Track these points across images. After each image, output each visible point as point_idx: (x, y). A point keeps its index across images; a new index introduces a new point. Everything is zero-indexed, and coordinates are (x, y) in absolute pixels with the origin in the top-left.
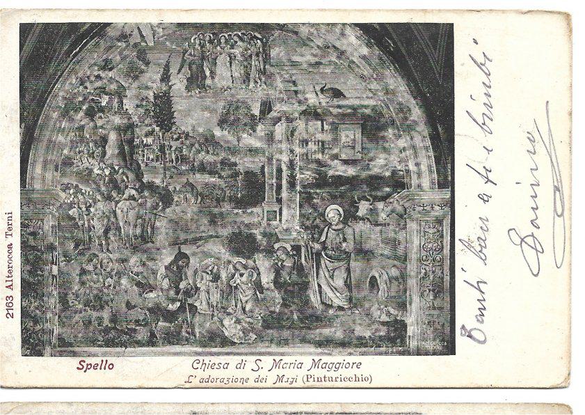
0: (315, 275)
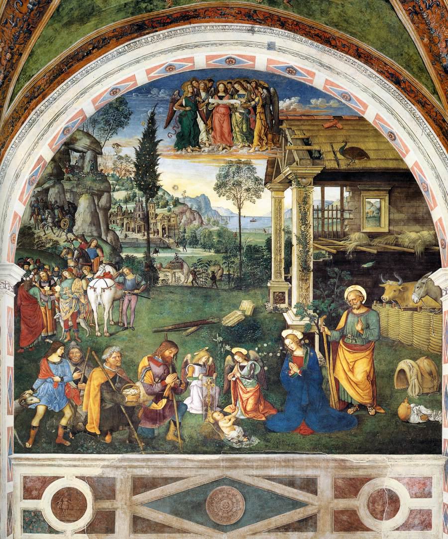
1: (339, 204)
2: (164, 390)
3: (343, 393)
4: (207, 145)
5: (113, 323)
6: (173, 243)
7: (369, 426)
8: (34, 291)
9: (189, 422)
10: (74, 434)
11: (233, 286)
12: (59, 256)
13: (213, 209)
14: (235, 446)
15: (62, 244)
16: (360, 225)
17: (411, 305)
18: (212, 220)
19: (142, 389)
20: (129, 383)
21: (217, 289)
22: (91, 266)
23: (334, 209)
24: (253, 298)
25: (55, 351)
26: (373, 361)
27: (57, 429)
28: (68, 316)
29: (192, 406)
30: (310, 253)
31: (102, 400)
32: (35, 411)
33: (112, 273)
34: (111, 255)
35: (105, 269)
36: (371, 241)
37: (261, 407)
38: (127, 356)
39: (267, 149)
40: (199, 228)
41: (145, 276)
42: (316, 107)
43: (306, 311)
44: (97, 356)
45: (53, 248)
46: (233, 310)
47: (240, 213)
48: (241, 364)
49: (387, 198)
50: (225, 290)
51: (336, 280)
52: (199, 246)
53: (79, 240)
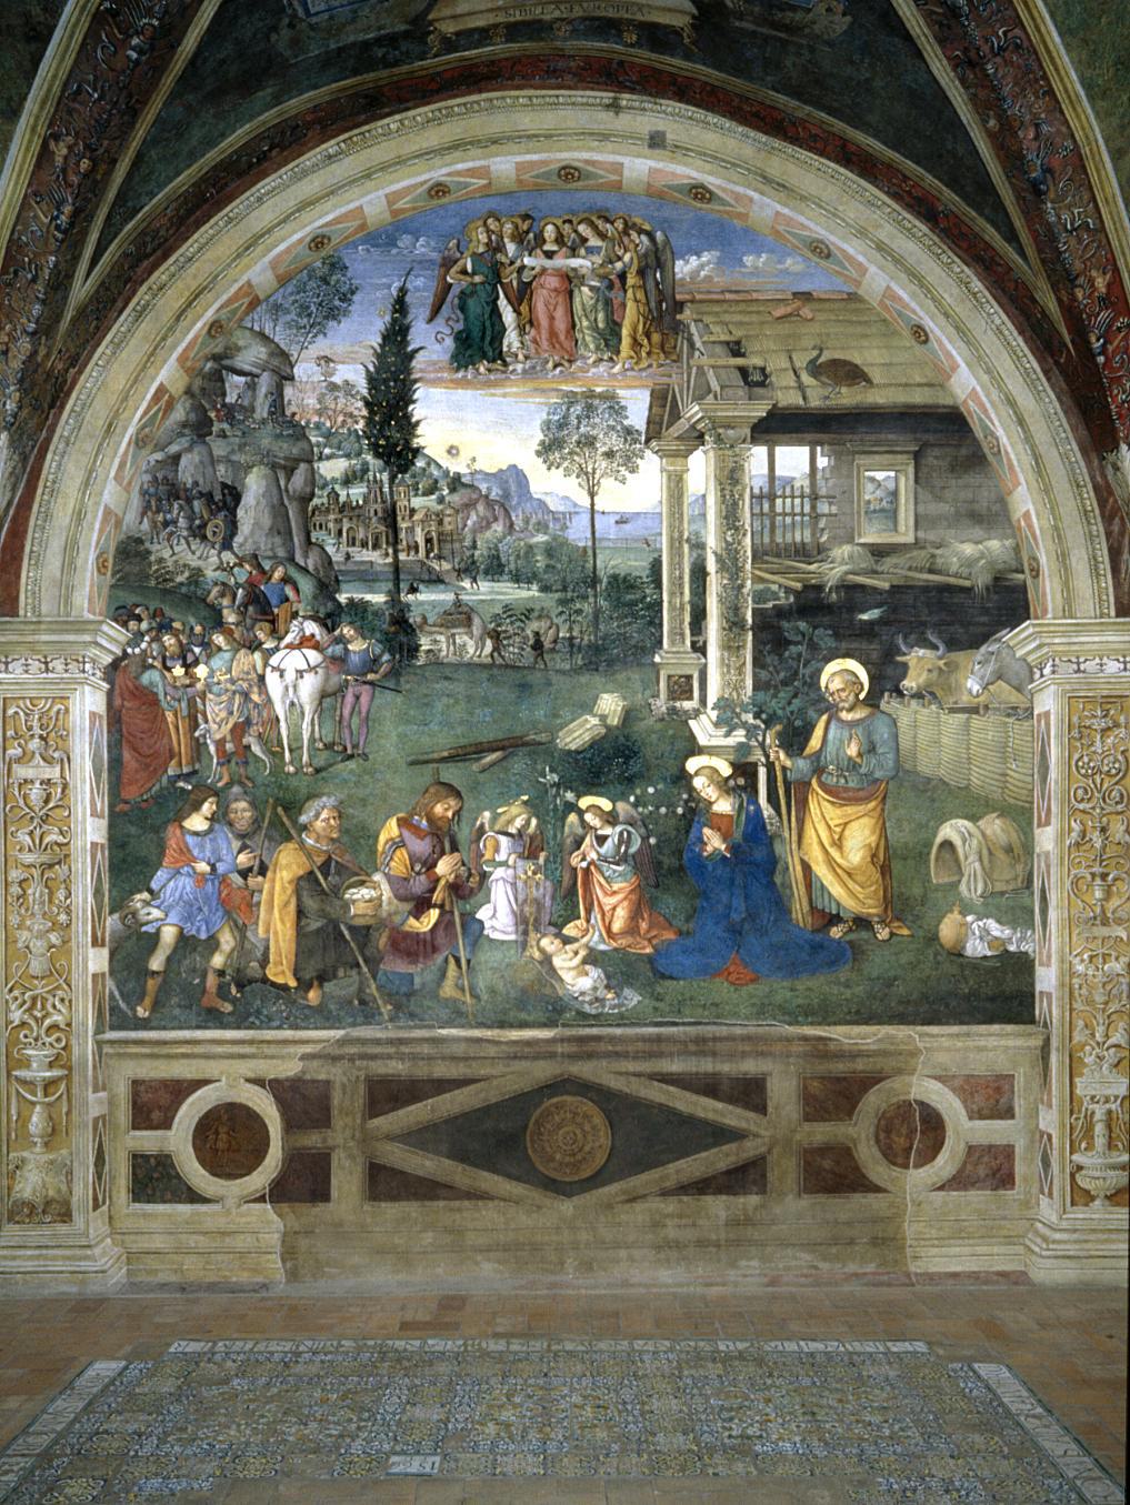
0: (794, 838)
1: (807, 483)
2: (432, 890)
3: (819, 893)
4: (521, 357)
5: (321, 746)
6: (448, 571)
7: (877, 963)
8: (149, 677)
9: (486, 957)
10: (240, 986)
11: (580, 662)
12: (204, 600)
13: (535, 496)
14: (587, 1009)
15: (210, 574)
17: (965, 700)
18: (533, 520)
19: (385, 887)
22: (273, 622)
23: (797, 493)
24: (619, 688)
25: (197, 807)
26: (884, 823)
27: (204, 976)
29: (494, 922)
30: (745, 591)
31: (301, 913)
32: (154, 940)
33: (318, 637)
34: (315, 597)
35: (302, 630)
36: (877, 562)
37: (644, 926)
38: (353, 817)
39: (650, 366)
40: (504, 537)
41: (389, 642)
42: (756, 272)
43: (738, 715)
44: (289, 817)
45: (189, 584)
46: (582, 715)
47: (593, 505)
48: (600, 832)
49: (911, 470)
50: (562, 672)
52: (506, 577)
53: (247, 567)
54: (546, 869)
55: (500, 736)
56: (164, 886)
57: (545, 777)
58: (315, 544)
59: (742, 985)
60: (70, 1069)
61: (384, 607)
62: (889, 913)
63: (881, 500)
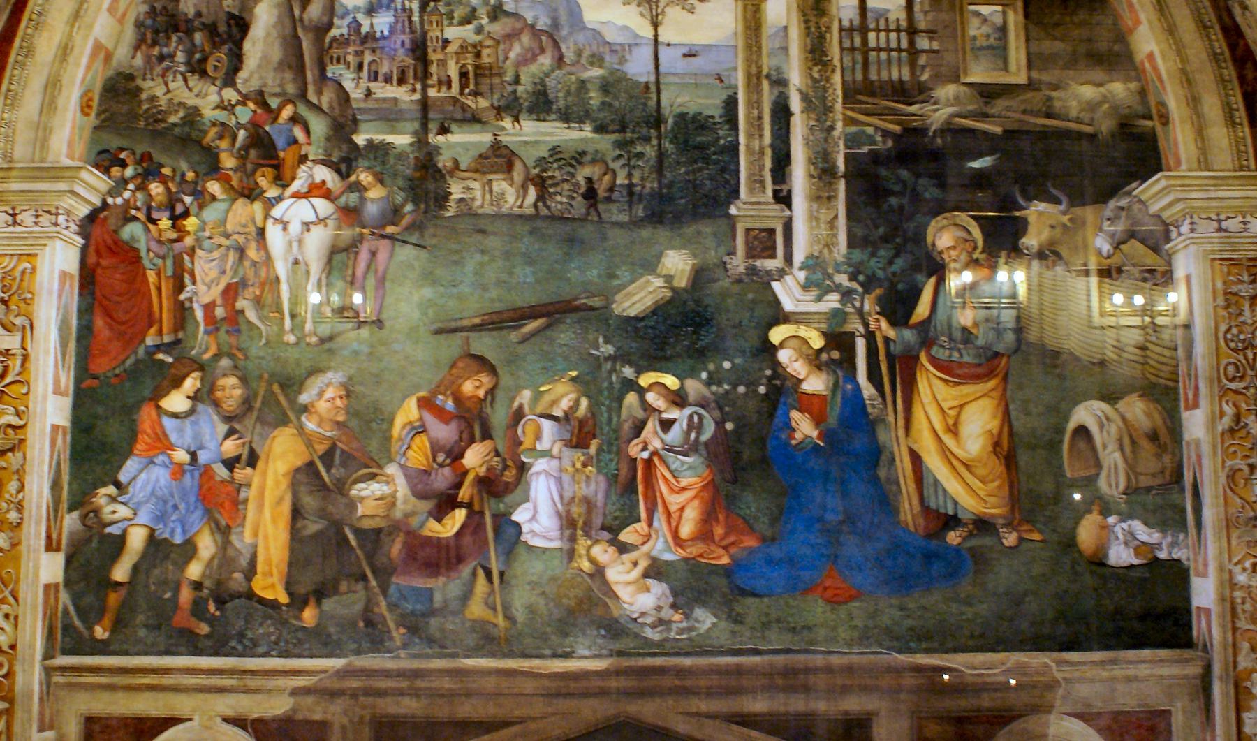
0: (901, 422)
1: (903, 16)
2: (458, 485)
3: (932, 490)
6: (485, 109)
7: (1003, 576)
8: (132, 232)
9: (528, 570)
10: (221, 602)
11: (641, 213)
14: (649, 633)
15: (209, 113)
16: (958, 68)
18: (586, 53)
20: (371, 469)
21: (600, 220)
22: (277, 167)
23: (892, 26)
25: (177, 383)
26: (1007, 406)
27: (177, 590)
28: (215, 293)
30: (836, 133)
31: (297, 513)
32: (120, 542)
33: (330, 185)
34: (328, 139)
35: (311, 176)
37: (719, 531)
40: (553, 71)
44: (286, 396)
45: (184, 124)
46: (642, 275)
47: (656, 36)
48: (665, 415)
50: (620, 225)
51: (905, 201)
52: (553, 116)
53: (251, 105)
54: (599, 461)
55: (545, 299)
56: (134, 479)
57: (597, 349)
58: (330, 79)
59: (839, 603)
60: (11, 701)
61: (409, 150)
62: (1017, 515)
63: (988, 36)
